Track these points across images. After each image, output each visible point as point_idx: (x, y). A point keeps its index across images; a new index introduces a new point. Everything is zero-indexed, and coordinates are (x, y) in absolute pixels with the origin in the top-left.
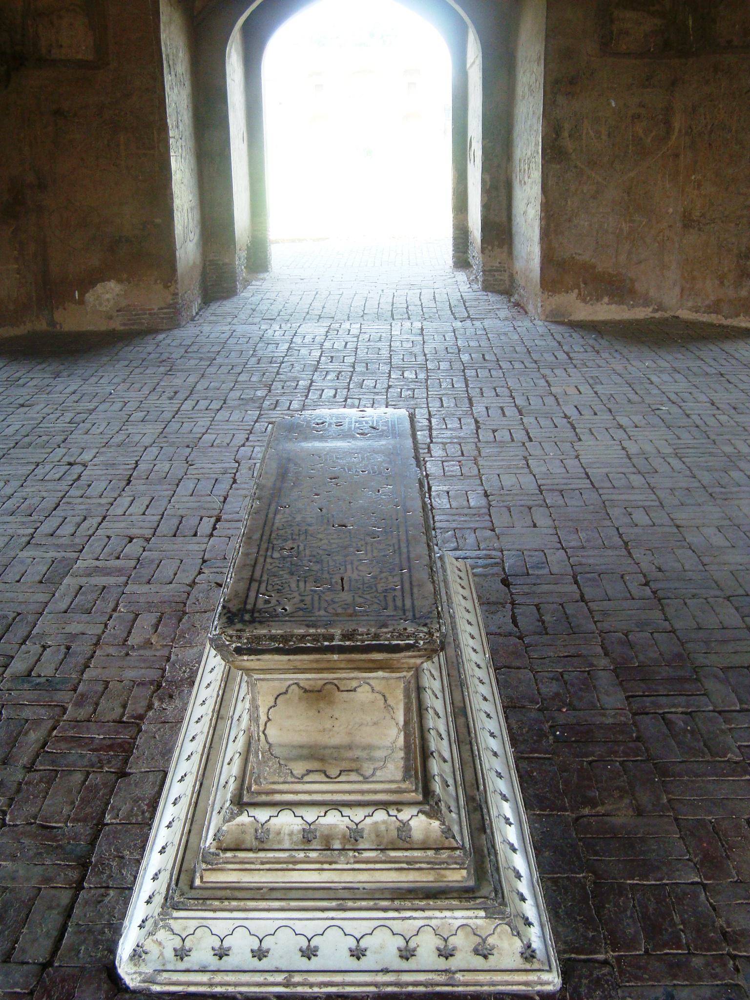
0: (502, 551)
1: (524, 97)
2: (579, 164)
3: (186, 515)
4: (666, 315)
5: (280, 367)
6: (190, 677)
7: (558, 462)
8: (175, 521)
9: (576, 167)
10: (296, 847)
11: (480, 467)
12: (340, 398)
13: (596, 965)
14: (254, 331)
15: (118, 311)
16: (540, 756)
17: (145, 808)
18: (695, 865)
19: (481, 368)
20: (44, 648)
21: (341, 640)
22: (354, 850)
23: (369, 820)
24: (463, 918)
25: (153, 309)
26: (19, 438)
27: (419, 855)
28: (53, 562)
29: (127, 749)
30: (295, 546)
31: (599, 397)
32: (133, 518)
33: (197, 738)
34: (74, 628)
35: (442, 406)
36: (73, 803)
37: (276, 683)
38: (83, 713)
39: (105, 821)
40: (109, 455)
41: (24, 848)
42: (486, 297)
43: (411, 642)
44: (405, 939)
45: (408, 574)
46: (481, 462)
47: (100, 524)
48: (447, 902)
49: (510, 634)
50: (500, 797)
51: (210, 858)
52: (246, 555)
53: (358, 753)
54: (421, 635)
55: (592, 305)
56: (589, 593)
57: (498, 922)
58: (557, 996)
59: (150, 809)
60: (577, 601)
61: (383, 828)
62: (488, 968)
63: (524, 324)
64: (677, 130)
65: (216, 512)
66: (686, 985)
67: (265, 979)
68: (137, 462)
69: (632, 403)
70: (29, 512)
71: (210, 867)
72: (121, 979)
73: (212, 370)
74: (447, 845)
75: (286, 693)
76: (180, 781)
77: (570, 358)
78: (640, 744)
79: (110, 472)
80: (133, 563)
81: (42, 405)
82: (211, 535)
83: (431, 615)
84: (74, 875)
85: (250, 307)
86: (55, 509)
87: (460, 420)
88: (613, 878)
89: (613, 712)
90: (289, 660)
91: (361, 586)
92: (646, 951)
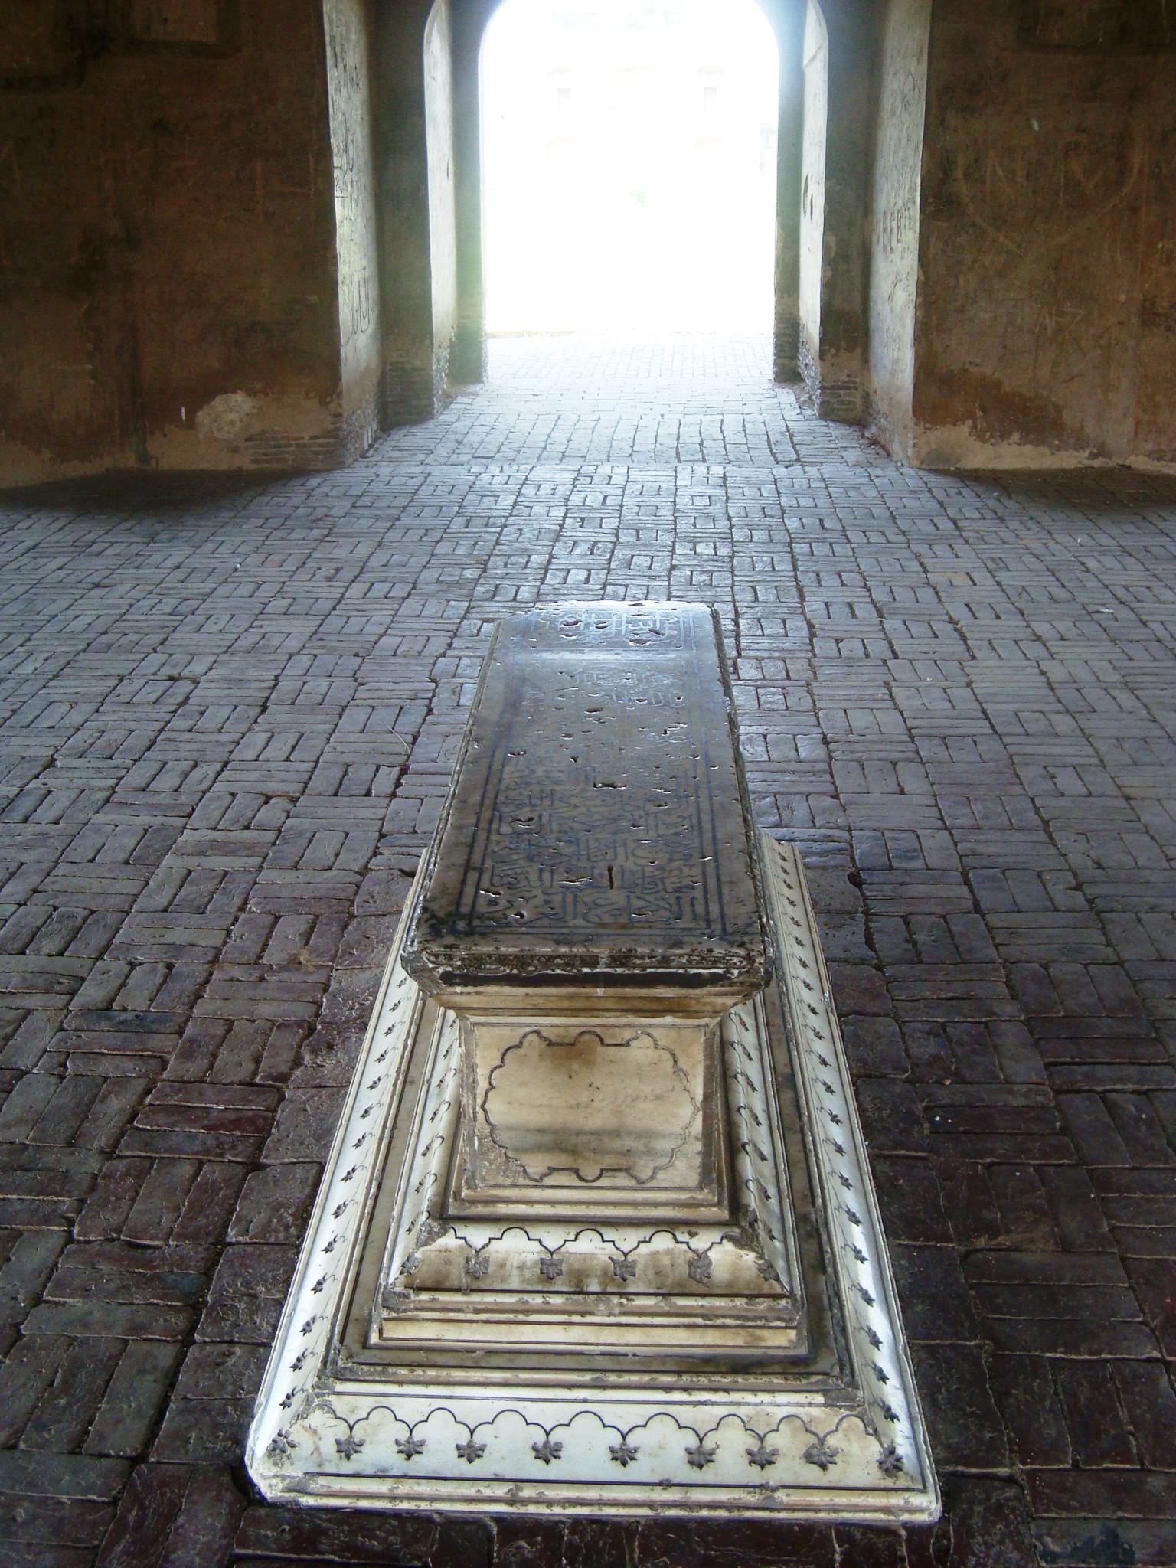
0: (850, 830)
1: (893, 113)
2: (978, 220)
3: (354, 763)
4: (1111, 464)
5: (500, 534)
6: (359, 1017)
7: (938, 693)
8: (336, 772)
9: (974, 225)
10: (529, 1288)
11: (815, 697)
12: (595, 584)
13: (997, 1484)
14: (460, 475)
15: (247, 440)
17: (290, 1219)
18: (1153, 1331)
19: (817, 541)
20: (132, 965)
21: (608, 966)
22: (621, 1295)
23: (644, 1249)
24: (789, 1404)
25: (303, 438)
26: (93, 636)
27: (723, 1304)
28: (146, 831)
29: (261, 1127)
30: (535, 815)
31: (1004, 591)
32: (271, 765)
33: (372, 1112)
34: (179, 936)
35: (756, 599)
36: (177, 1209)
37: (506, 1031)
38: (192, 1070)
39: (228, 1240)
40: (234, 665)
41: (102, 1277)
42: (825, 430)
43: (720, 971)
44: (698, 1435)
45: (713, 865)
46: (817, 689)
47: (219, 774)
48: (765, 1379)
49: (863, 961)
50: (846, 1216)
51: (393, 1301)
52: (459, 828)
53: (629, 1143)
54: (735, 960)
55: (993, 445)
56: (987, 899)
57: (844, 1412)
58: (935, 1530)
61: (666, 1260)
62: (828, 1485)
63: (884, 473)
64: (1135, 170)
65: (401, 759)
66: (1137, 1519)
67: (479, 1491)
68: (276, 678)
69: (1056, 602)
70: (108, 752)
71: (394, 1315)
72: (253, 1485)
73: (393, 535)
74: (766, 1290)
75: (519, 1046)
76: (346, 1179)
77: (958, 528)
78: (1066, 1139)
79: (235, 692)
80: (271, 836)
81: (128, 586)
82: (393, 795)
83: (753, 930)
84: (180, 1321)
85: (453, 437)
86: (148, 749)
87: (784, 621)
88: (1024, 1349)
89: (1024, 1089)
90: (527, 994)
91: (640, 881)
92: (1075, 1465)
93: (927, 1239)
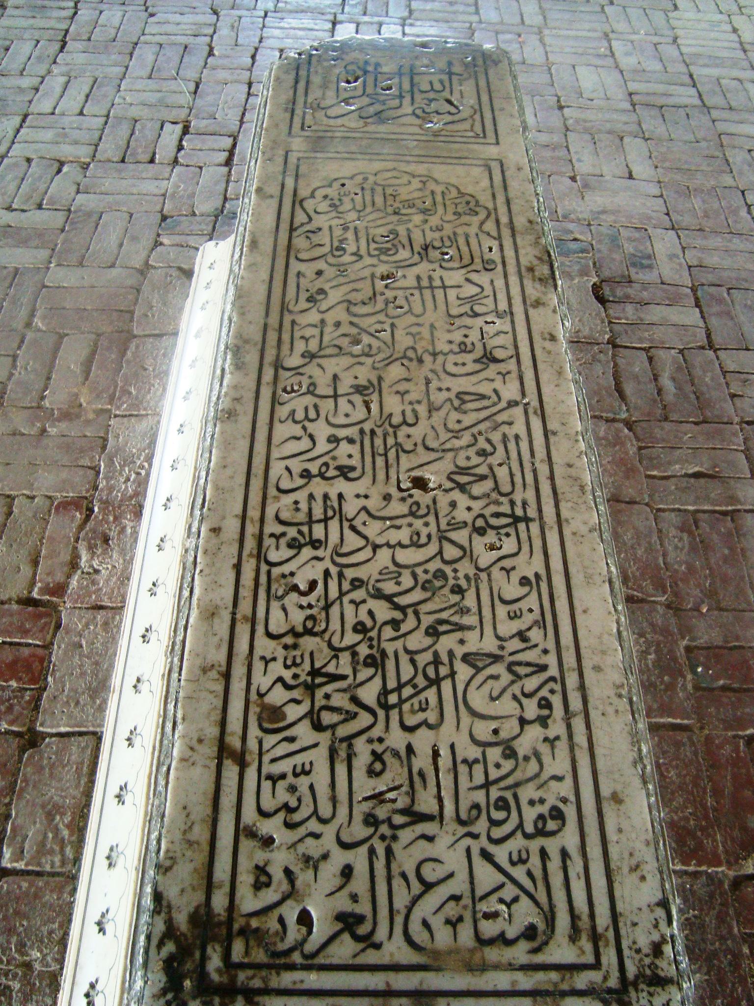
6: (136, 494)
7: (650, 49)
8: (124, 131)
11: (548, 49)
16: (674, 721)
17: (66, 833)
32: (66, 121)
47: (18, 131)
59: (74, 838)
60: (703, 348)
65: (182, 114)
79: (40, 23)
93: (699, 864)
